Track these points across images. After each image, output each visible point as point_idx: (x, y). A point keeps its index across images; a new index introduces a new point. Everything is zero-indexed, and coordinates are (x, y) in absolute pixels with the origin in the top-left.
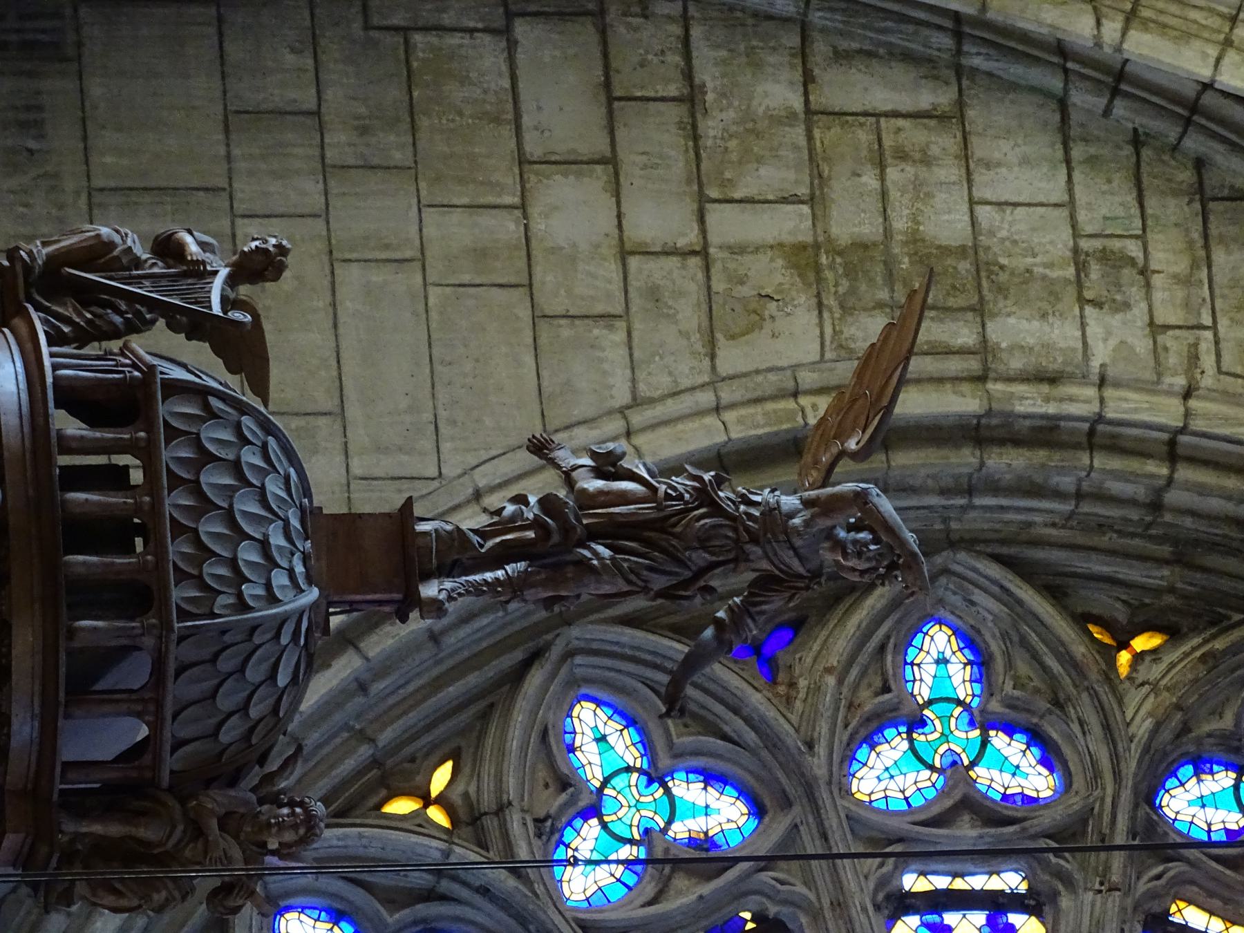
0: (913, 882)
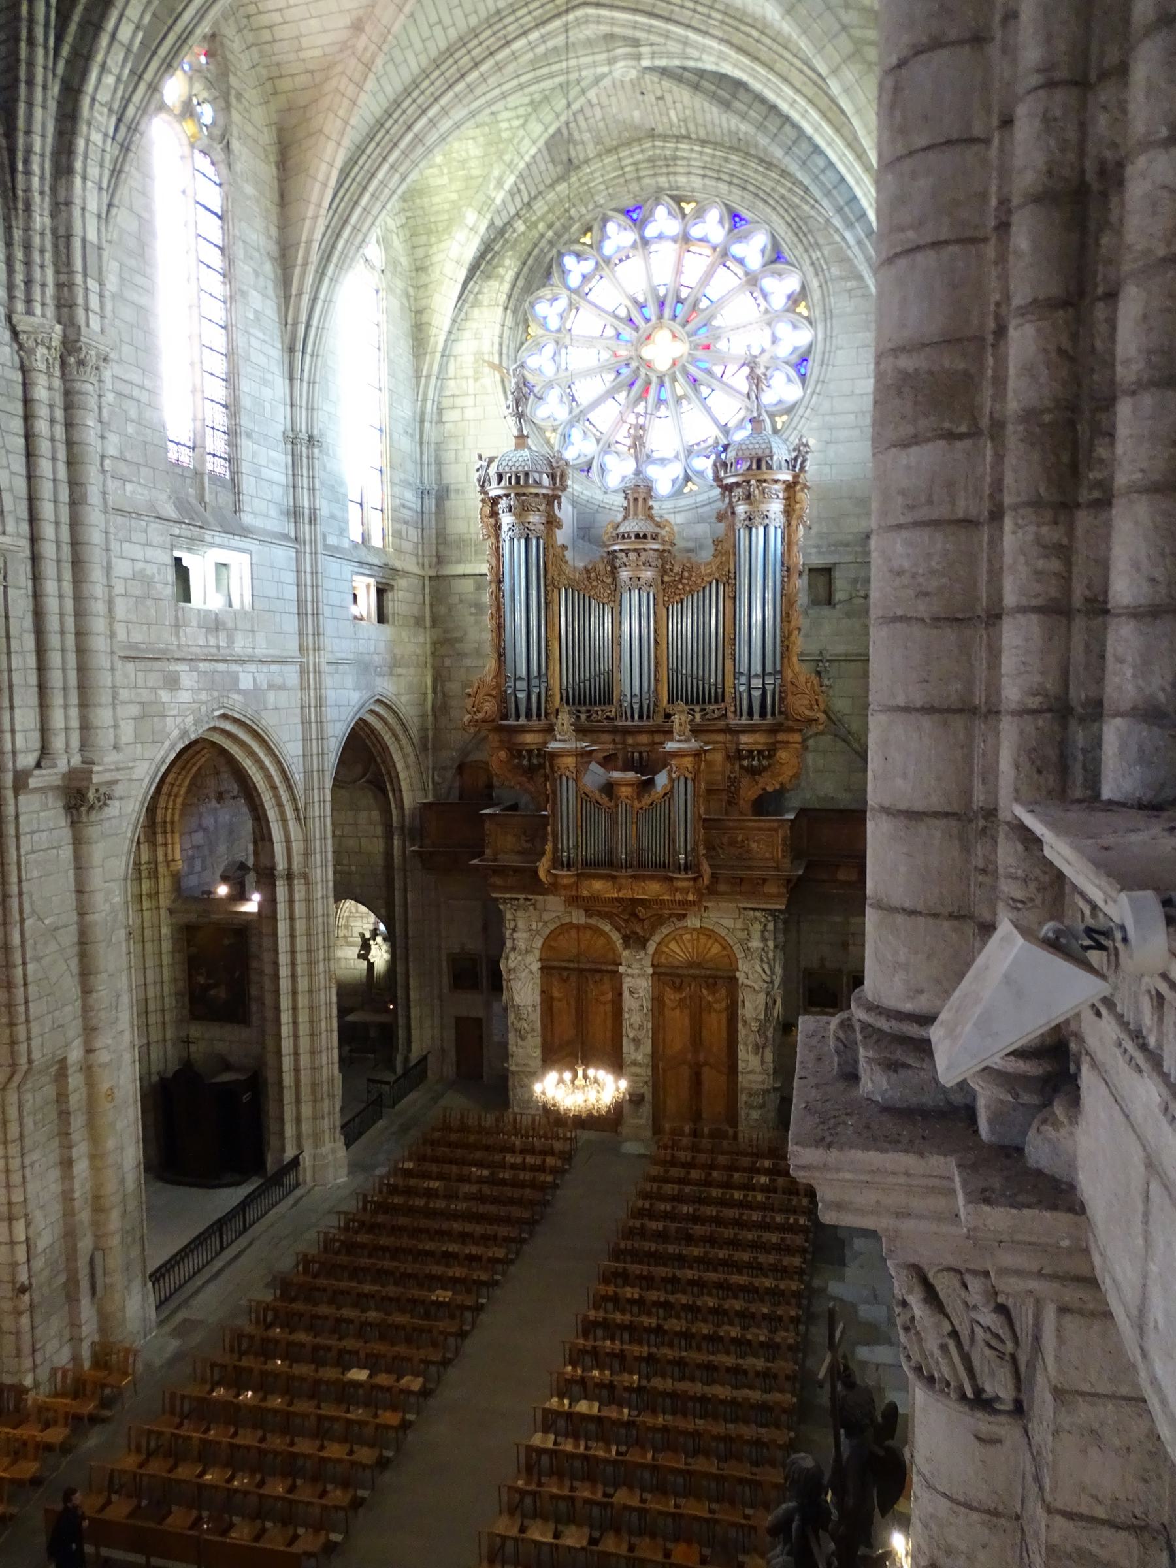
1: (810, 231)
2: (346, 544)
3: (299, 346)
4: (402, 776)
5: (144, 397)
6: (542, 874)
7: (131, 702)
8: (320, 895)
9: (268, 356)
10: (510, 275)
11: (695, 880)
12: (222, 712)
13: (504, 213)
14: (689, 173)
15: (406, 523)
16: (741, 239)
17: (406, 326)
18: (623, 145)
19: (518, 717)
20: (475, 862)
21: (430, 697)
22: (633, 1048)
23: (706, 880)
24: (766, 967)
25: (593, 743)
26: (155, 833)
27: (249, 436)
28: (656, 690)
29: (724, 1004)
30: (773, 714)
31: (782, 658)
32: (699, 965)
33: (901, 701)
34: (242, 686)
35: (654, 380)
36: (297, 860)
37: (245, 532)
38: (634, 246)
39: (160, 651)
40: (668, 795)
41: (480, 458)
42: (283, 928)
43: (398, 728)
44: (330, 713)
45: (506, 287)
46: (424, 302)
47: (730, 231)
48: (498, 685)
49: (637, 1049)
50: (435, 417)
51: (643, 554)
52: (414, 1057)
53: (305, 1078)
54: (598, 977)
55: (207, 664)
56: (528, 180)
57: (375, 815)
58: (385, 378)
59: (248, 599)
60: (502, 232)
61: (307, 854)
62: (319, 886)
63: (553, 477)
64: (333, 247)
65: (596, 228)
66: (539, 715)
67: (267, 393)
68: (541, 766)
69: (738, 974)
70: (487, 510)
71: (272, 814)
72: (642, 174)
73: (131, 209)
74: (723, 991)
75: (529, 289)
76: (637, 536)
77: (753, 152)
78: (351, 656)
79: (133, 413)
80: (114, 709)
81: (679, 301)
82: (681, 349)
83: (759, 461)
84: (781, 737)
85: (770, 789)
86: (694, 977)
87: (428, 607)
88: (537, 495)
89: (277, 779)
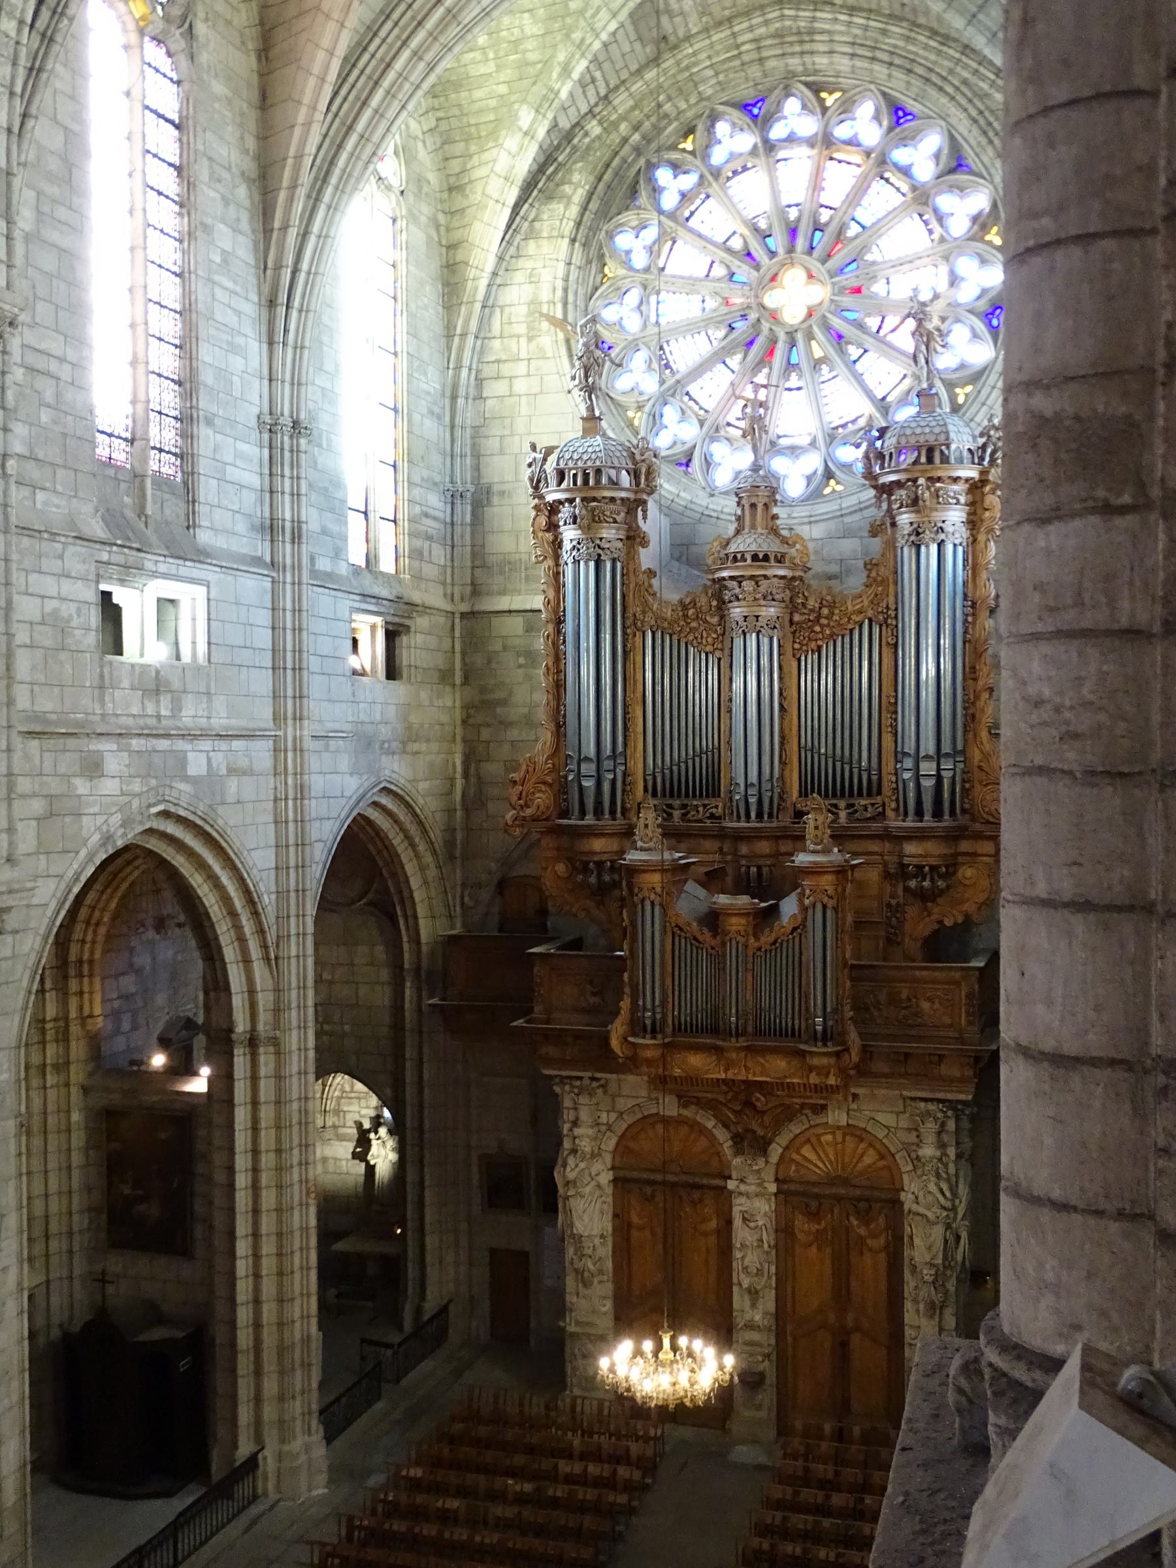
0: (653, 319)
2: (343, 569)
3: (283, 298)
4: (418, 896)
5: (65, 372)
6: (615, 1043)
7: (34, 795)
8: (295, 1069)
9: (239, 313)
10: (579, 196)
11: (838, 1055)
12: (161, 808)
13: (573, 109)
14: (831, 52)
15: (429, 538)
16: (904, 141)
17: (434, 266)
18: (738, 15)
19: (583, 813)
20: (519, 1023)
21: (459, 783)
22: (747, 1303)
23: (855, 1056)
24: (945, 1187)
25: (691, 852)
26: (66, 977)
27: (209, 422)
28: (782, 777)
29: (882, 1241)
30: (953, 813)
31: (965, 732)
32: (846, 1182)
33: (1041, 890)
34: (192, 771)
35: (782, 336)
36: (264, 1018)
37: (201, 556)
38: (754, 152)
39: (78, 724)
40: (799, 929)
41: (534, 447)
42: (241, 1116)
43: (413, 829)
44: (314, 807)
45: (574, 211)
46: (457, 235)
47: (890, 130)
48: (554, 769)
49: (754, 1305)
50: (472, 391)
51: (764, 584)
52: (430, 1306)
53: (269, 1338)
54: (696, 1195)
55: (142, 741)
56: (606, 66)
57: (380, 951)
58: (402, 338)
59: (202, 648)
60: (569, 136)
61: (278, 1010)
62: (295, 1058)
63: (635, 474)
64: (332, 163)
65: (700, 128)
66: (613, 812)
67: (237, 363)
68: (615, 885)
69: (903, 1195)
70: (543, 521)
71: (230, 953)
72: (765, 54)
73: (55, 119)
74: (881, 1221)
75: (605, 214)
76: (755, 558)
77: (922, 20)
78: (348, 727)
79: (49, 396)
80: (10, 805)
81: (818, 227)
82: (819, 293)
83: (930, 451)
84: (965, 846)
85: (948, 922)
86: (839, 1199)
87: (458, 656)
88: (613, 500)
89: (238, 903)
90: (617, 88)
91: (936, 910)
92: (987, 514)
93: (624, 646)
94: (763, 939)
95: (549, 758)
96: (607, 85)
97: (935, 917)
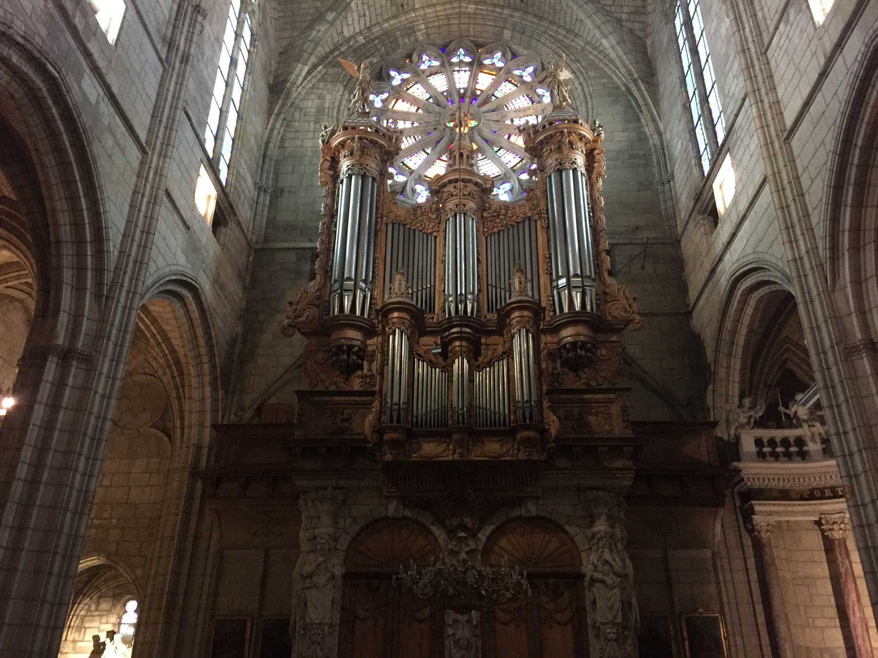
1: (571, 53)
13: (351, 28)
50: (278, 143)
56: (372, 9)
60: (348, 40)
90: (375, 25)
91: (583, 376)
92: (596, 164)
93: (376, 227)
94: (480, 359)
95: (317, 291)
96: (371, 21)
97: (584, 381)
